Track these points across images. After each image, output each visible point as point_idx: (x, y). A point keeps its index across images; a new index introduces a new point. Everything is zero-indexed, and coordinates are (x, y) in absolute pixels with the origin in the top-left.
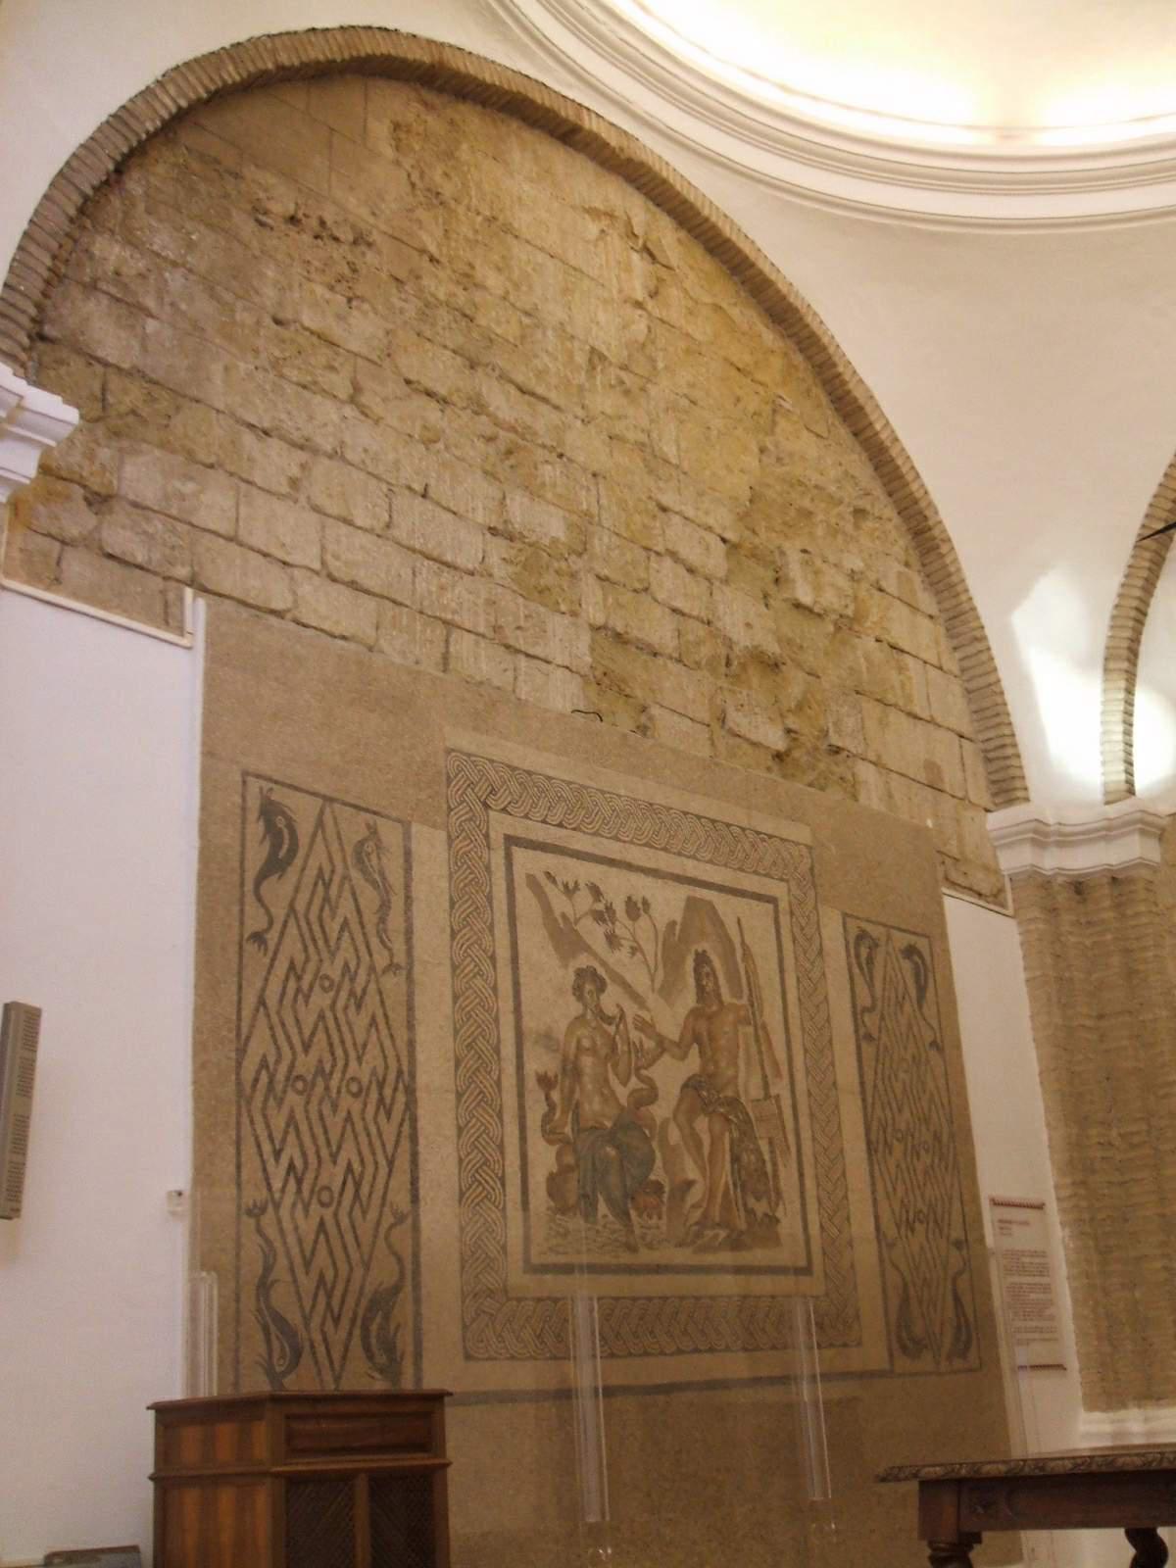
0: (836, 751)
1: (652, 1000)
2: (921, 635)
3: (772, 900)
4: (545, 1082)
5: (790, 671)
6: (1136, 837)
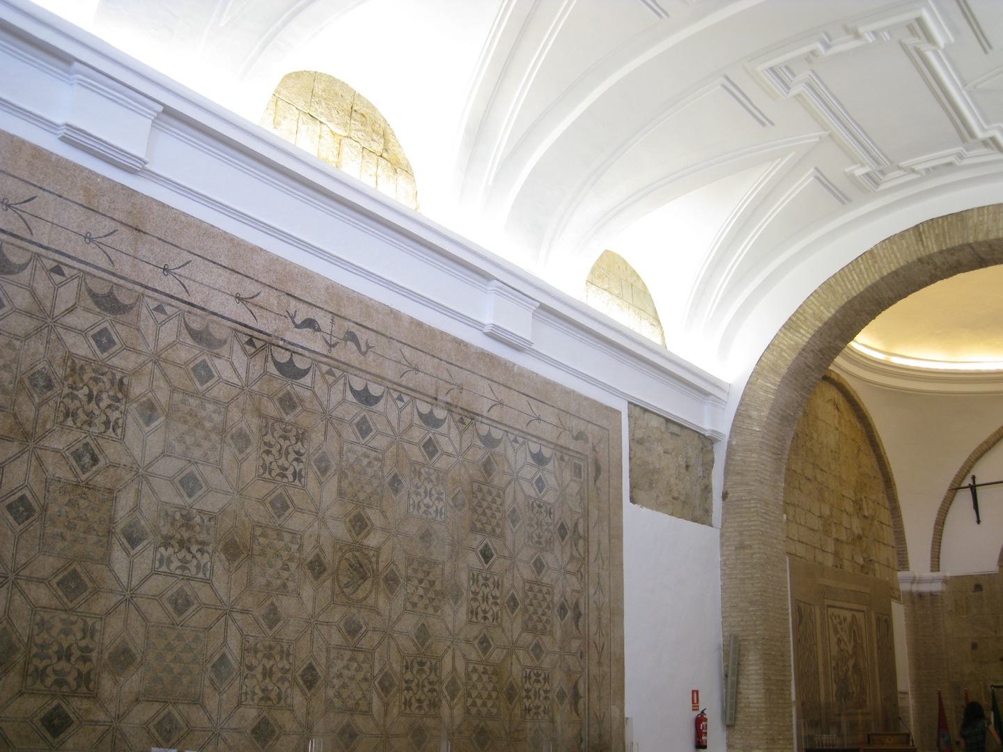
0: (871, 560)
1: (848, 643)
2: (885, 515)
3: (863, 611)
4: (834, 668)
5: (864, 539)
6: (940, 584)
